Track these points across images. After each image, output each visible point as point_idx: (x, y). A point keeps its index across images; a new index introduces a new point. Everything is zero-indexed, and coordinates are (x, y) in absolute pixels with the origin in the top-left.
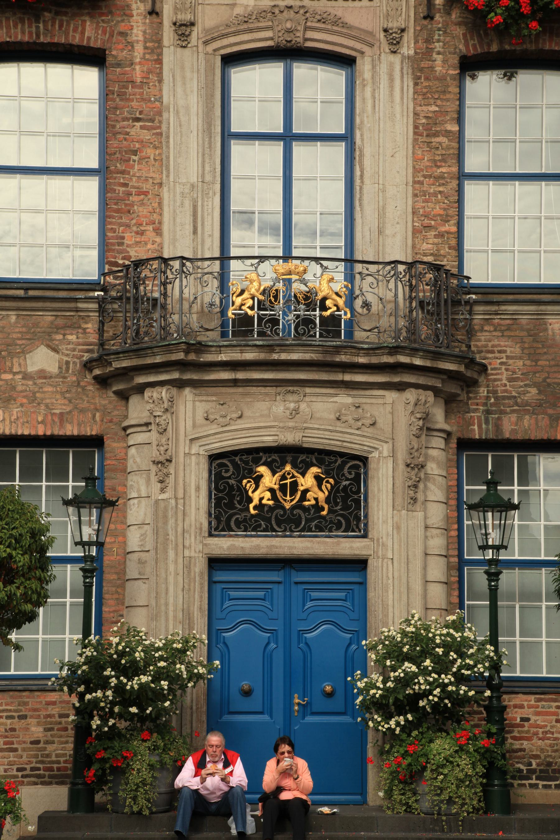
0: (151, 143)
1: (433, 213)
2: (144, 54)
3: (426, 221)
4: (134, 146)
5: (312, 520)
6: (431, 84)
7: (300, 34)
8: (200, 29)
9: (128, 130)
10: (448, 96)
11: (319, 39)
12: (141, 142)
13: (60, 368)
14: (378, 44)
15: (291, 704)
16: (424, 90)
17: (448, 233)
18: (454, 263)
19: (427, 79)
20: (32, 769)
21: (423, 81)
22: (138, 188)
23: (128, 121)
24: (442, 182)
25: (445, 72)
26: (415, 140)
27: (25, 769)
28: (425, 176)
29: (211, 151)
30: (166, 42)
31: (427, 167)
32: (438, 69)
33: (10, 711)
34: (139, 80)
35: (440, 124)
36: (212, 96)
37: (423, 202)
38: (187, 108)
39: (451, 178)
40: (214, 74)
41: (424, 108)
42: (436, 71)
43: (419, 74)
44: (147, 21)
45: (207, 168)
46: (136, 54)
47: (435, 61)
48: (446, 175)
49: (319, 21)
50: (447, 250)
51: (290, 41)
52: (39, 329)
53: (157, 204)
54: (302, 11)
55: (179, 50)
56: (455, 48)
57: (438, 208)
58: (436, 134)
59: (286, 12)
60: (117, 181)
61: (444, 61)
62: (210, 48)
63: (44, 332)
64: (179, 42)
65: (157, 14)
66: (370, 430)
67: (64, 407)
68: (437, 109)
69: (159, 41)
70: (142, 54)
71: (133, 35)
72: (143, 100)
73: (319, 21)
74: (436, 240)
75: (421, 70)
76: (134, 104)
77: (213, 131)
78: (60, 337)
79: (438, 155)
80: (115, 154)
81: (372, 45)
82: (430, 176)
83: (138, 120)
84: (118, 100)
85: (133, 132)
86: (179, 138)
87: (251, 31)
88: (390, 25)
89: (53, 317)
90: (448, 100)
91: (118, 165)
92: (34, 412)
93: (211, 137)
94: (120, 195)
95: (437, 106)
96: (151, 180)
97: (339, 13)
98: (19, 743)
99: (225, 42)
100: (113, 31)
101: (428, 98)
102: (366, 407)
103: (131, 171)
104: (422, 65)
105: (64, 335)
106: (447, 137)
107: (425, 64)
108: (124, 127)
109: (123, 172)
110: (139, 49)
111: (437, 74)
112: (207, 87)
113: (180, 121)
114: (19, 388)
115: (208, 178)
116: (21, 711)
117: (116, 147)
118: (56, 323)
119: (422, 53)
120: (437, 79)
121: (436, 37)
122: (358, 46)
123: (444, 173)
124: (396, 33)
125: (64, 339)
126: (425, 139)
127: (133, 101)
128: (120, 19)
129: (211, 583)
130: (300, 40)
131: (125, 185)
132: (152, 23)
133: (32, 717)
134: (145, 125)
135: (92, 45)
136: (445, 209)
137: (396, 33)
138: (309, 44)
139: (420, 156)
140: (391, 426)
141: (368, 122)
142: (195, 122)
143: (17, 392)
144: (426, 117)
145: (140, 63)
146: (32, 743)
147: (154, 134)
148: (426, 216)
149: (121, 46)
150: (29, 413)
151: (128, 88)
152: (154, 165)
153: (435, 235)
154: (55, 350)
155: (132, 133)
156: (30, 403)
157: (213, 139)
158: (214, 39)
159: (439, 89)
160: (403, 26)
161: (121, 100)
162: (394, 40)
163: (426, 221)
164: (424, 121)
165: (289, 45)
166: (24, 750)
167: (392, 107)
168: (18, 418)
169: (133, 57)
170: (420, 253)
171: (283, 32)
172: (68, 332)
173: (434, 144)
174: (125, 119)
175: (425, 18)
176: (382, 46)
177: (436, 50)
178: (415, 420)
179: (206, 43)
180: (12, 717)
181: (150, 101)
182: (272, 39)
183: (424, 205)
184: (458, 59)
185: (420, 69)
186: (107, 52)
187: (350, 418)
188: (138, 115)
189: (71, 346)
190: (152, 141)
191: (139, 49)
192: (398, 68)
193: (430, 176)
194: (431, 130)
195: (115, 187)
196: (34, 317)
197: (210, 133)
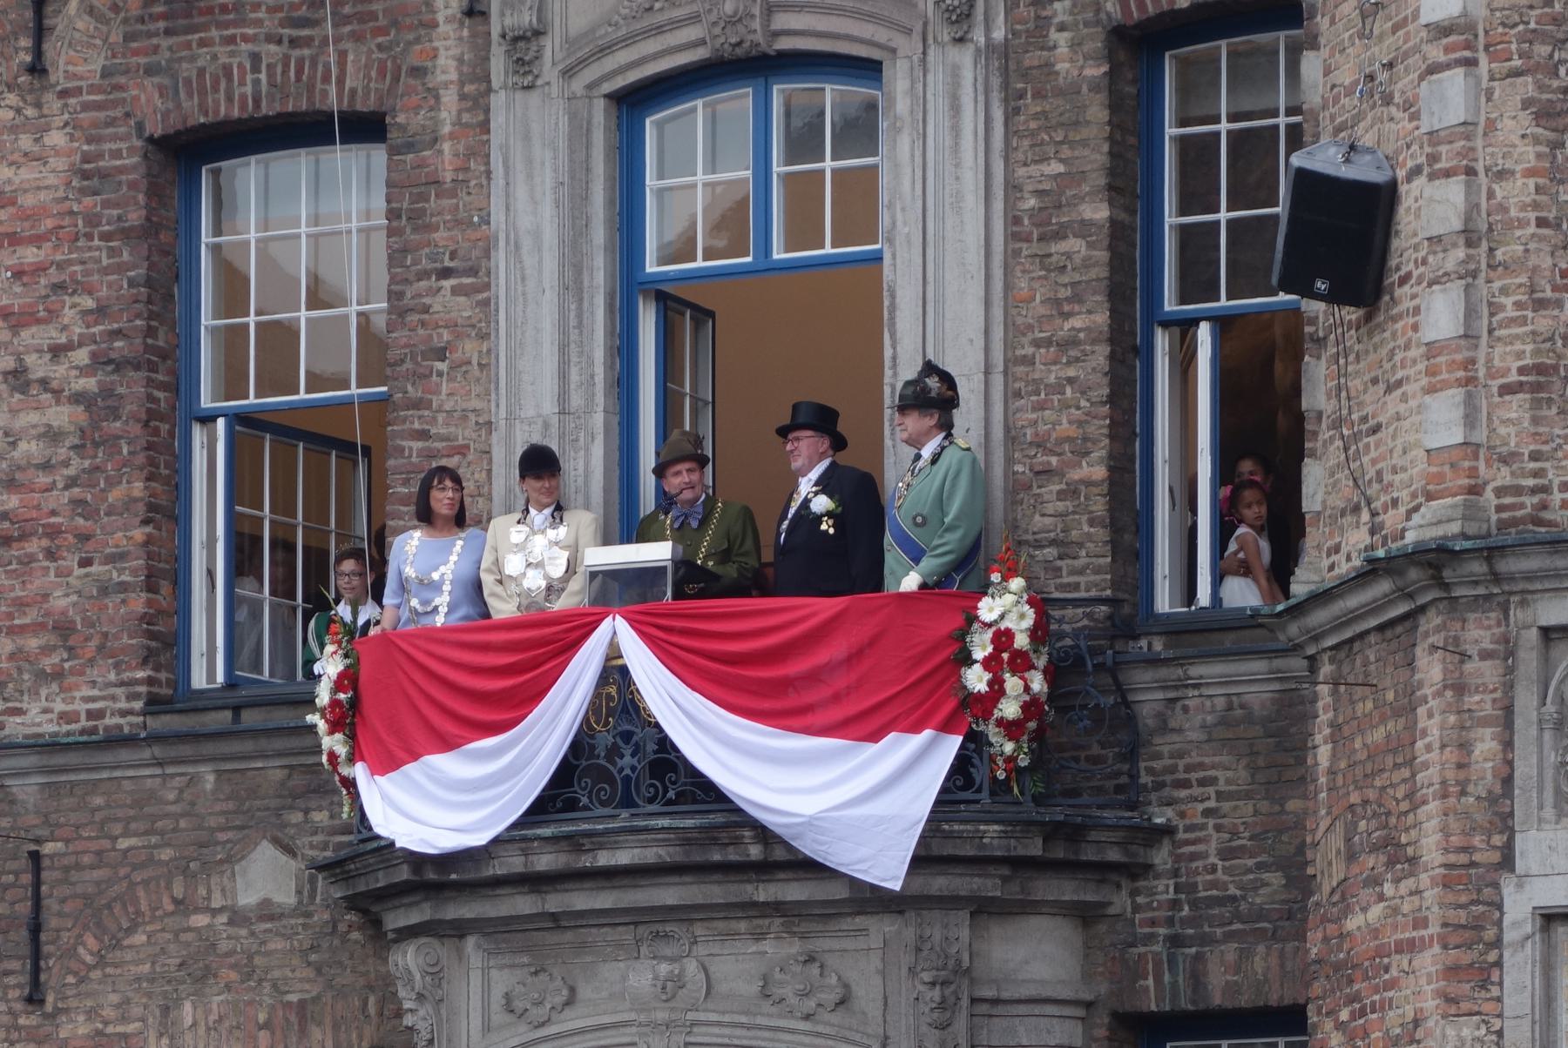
0: (473, 326)
1: (1054, 435)
2: (460, 112)
3: (1041, 458)
4: (440, 336)
6: (1048, 107)
7: (756, 24)
9: (427, 300)
10: (1085, 133)
12: (452, 325)
13: (299, 892)
14: (918, 27)
16: (1033, 125)
17: (1089, 483)
18: (1101, 561)
19: (1038, 95)
22: (448, 439)
23: (429, 278)
24: (1073, 353)
25: (1076, 73)
26: (1011, 256)
28: (1037, 344)
29: (581, 333)
30: (497, 79)
31: (1040, 319)
32: (1062, 67)
34: (448, 177)
35: (1069, 205)
36: (586, 198)
37: (1034, 409)
38: (537, 234)
39: (1094, 342)
40: (588, 146)
41: (1034, 170)
42: (1057, 73)
43: (1020, 86)
44: (465, 33)
45: (574, 376)
46: (444, 114)
47: (1055, 47)
48: (1082, 335)
50: (1086, 528)
51: (739, 44)
52: (258, 802)
53: (484, 474)
55: (519, 95)
56: (1098, 11)
57: (1064, 421)
58: (1059, 235)
60: (407, 426)
61: (1074, 45)
62: (578, 85)
63: (268, 809)
65: (483, 14)
66: (835, 1018)
67: (307, 987)
68: (1061, 168)
70: (454, 113)
71: (438, 72)
72: (458, 222)
74: (1061, 506)
76: (440, 236)
77: (586, 283)
78: (297, 817)
79: (1065, 285)
80: (403, 361)
81: (908, 32)
82: (1048, 342)
83: (446, 273)
84: (408, 230)
85: (437, 304)
86: (520, 308)
87: (659, 30)
89: (286, 771)
90: (1084, 143)
91: (410, 388)
92: (250, 1003)
93: (581, 300)
94: (414, 459)
95: (1061, 161)
100: (399, 68)
101: (1042, 143)
102: (831, 961)
103: (434, 398)
104: (1027, 63)
105: (306, 812)
106: (1084, 237)
107: (1033, 58)
108: (420, 296)
109: (417, 405)
110: (449, 98)
111: (1061, 80)
112: (572, 178)
113: (522, 269)
114: (224, 946)
115: (576, 400)
117: (406, 346)
118: (291, 783)
119: (1027, 31)
120: (1060, 92)
123: (1079, 330)
125: (306, 821)
126: (1036, 248)
127: (437, 229)
128: (411, 37)
130: (759, 37)
131: (423, 435)
132: (473, 35)
134: (460, 285)
135: (359, 107)
136: (1080, 423)
138: (785, 44)
139: (1025, 293)
140: (880, 1003)
141: (905, 224)
142: (546, 267)
143: (218, 956)
144: (1039, 193)
145: (452, 136)
147: (479, 303)
148: (1040, 444)
149: (415, 99)
150: (241, 1005)
151: (428, 201)
152: (478, 380)
153: (1059, 492)
154: (290, 851)
155: (436, 307)
156: (243, 982)
157: (586, 304)
158: (583, 63)
161: (415, 230)
163: (1041, 458)
164: (1032, 202)
165: (739, 52)
167: (957, 178)
168: (221, 1019)
169: (437, 123)
170: (1027, 542)
172: (313, 804)
173: (1054, 259)
174: (423, 275)
176: (930, 28)
178: (921, 988)
179: (568, 73)
181: (471, 222)
183: (1034, 416)
184: (1103, 37)
185: (1016, 76)
186: (388, 120)
187: (787, 992)
188: (448, 263)
189: (319, 838)
190: (474, 321)
191: (449, 98)
192: (968, 76)
193: (1048, 342)
194: (1050, 224)
195: (404, 443)
196: (250, 774)
197: (580, 290)
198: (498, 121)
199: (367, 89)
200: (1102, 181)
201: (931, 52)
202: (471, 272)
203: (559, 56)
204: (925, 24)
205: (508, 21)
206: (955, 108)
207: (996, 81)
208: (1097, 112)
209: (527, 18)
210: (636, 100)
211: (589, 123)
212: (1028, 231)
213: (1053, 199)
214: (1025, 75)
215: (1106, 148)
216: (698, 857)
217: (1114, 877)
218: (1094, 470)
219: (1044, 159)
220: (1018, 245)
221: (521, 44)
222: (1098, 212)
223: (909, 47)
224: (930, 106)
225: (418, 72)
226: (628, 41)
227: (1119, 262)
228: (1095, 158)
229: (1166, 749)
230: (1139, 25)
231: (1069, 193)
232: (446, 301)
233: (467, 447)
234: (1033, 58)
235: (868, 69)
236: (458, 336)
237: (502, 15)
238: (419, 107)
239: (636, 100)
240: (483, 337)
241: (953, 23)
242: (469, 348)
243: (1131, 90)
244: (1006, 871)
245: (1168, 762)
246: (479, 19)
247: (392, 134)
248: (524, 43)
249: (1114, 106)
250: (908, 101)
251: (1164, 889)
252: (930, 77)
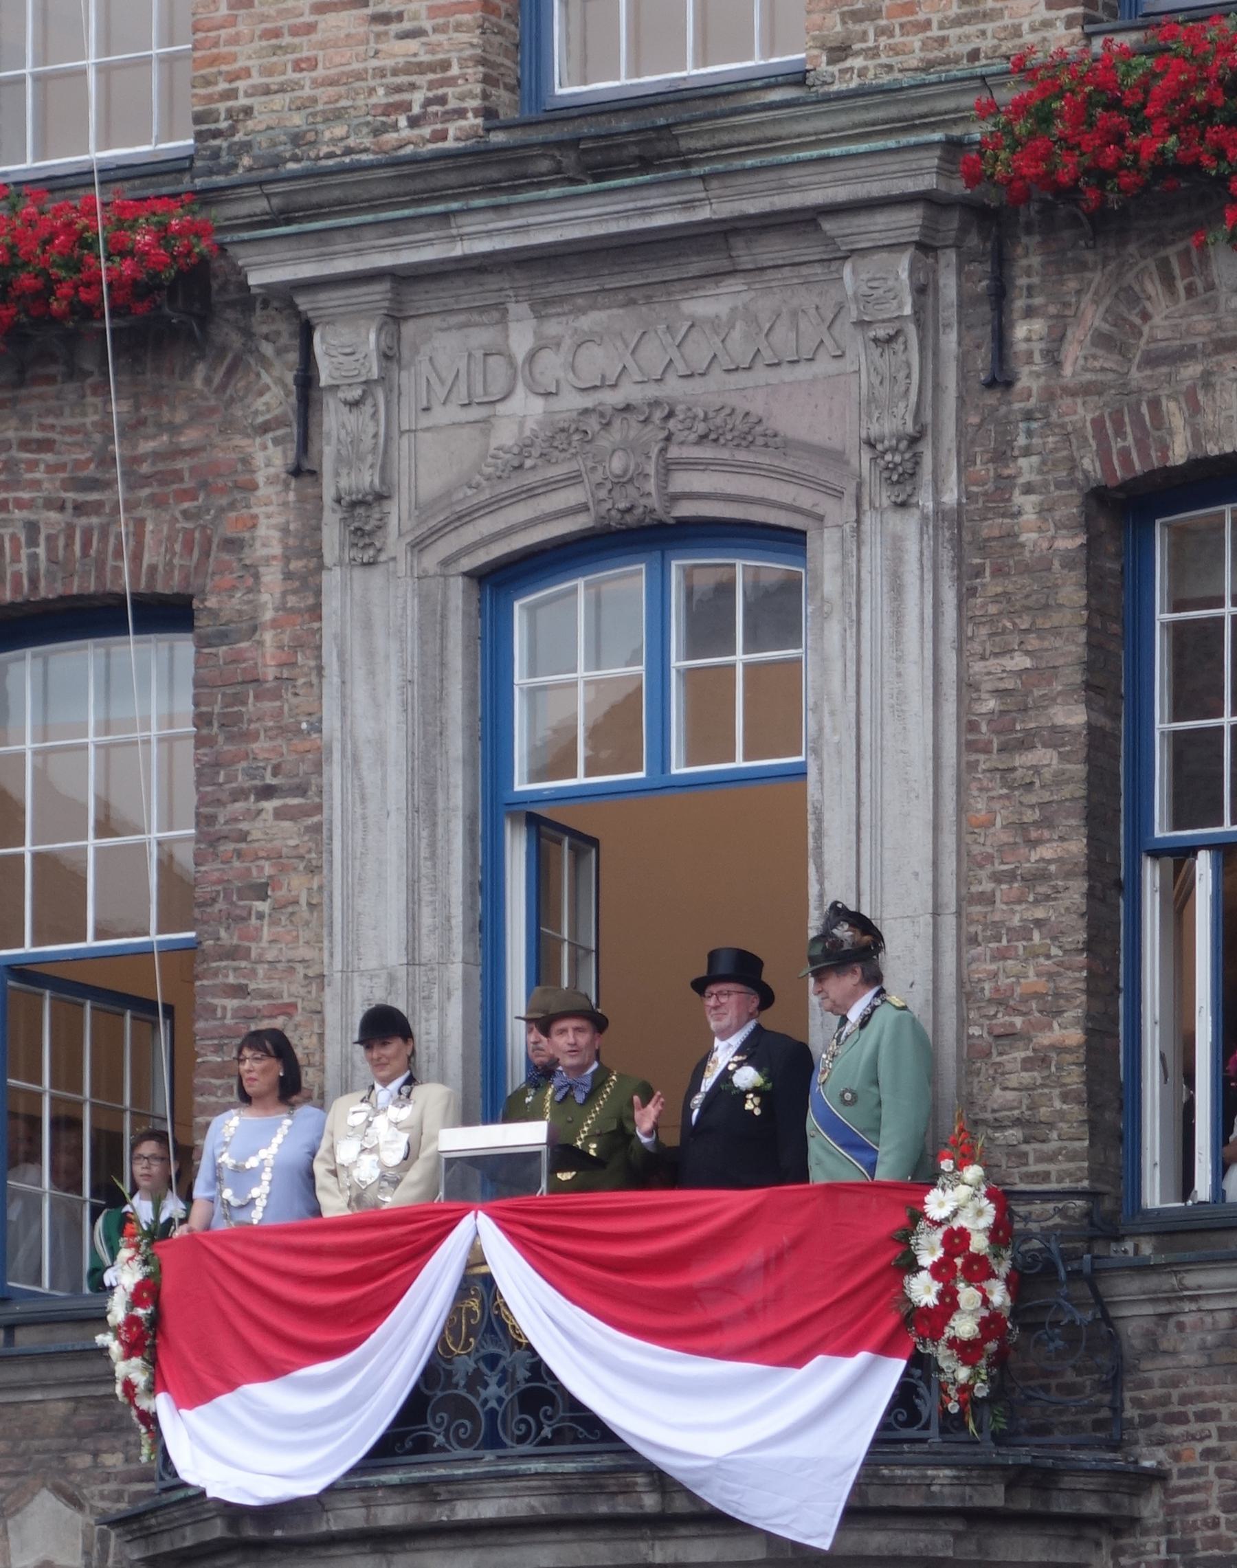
0: (302, 857)
1: (1018, 990)
2: (284, 594)
3: (1002, 1019)
4: (261, 869)
6: (1010, 588)
7: (651, 486)
8: (405, 506)
9: (244, 826)
10: (1056, 619)
11: (709, 487)
12: (276, 857)
13: (87, 1553)
14: (851, 489)
16: (993, 609)
17: (1061, 1049)
18: (1077, 1144)
19: (998, 572)
21: (987, 579)
23: (247, 799)
24: (1042, 889)
25: (1045, 545)
26: (966, 770)
28: (997, 878)
29: (434, 866)
30: (330, 553)
31: (1001, 848)
32: (1028, 537)
34: (271, 673)
35: (1037, 708)
36: (440, 699)
37: (994, 959)
38: (379, 744)
39: (1068, 875)
40: (443, 636)
41: (993, 664)
42: (1022, 546)
43: (978, 561)
44: (292, 496)
45: (426, 919)
46: (265, 597)
47: (1020, 513)
48: (1053, 868)
50: (1058, 1104)
51: (629, 510)
52: (37, 1443)
53: (315, 1039)
54: (658, 415)
55: (358, 573)
56: (1073, 469)
57: (1031, 973)
58: (1024, 744)
59: (617, 423)
60: (220, 980)
61: (1044, 511)
62: (430, 561)
65: (313, 473)
68: (1027, 663)
69: (317, 552)
70: (278, 595)
71: (258, 544)
72: (282, 730)
74: (1026, 1077)
75: (982, 547)
76: (260, 746)
77: (441, 805)
78: (84, 1461)
79: (1032, 807)
80: (214, 900)
81: (838, 494)
82: (1011, 876)
83: (267, 792)
84: (221, 739)
85: (256, 829)
86: (359, 835)
87: (530, 493)
88: (875, 430)
89: (71, 1405)
90: (1056, 631)
91: (223, 933)
93: (434, 824)
94: (229, 1021)
95: (1027, 653)
96: (300, 969)
97: (757, 407)
99: (470, 534)
100: (209, 541)
101: (1004, 630)
103: (253, 945)
104: (985, 533)
105: (96, 1454)
106: (1055, 747)
107: (992, 527)
108: (236, 820)
109: (233, 953)
110: (272, 577)
111: (1027, 554)
112: (423, 675)
113: (362, 787)
115: (429, 949)
117: (220, 882)
118: (76, 1419)
119: (985, 494)
120: (1026, 569)
121: (1022, 441)
123: (1049, 862)
124: (894, 450)
125: (96, 1465)
126: (996, 760)
127: (255, 737)
128: (224, 501)
130: (654, 502)
131: (239, 991)
132: (302, 499)
134: (285, 806)
135: (160, 588)
136: (1051, 976)
137: (894, 450)
138: (686, 510)
139: (982, 816)
141: (834, 730)
142: (391, 785)
144: (999, 693)
145: (275, 624)
147: (308, 829)
148: (1001, 1001)
149: (229, 578)
151: (244, 703)
152: (307, 923)
153: (1024, 1060)
154: (74, 1501)
155: (256, 835)
157: (440, 830)
158: (436, 533)
159: (1030, 602)
160: (910, 428)
161: (230, 738)
162: (901, 468)
163: (1002, 1019)
164: (991, 704)
165: (629, 519)
167: (899, 675)
169: (257, 607)
170: (984, 1122)
171: (609, 486)
172: (104, 1445)
174: (239, 795)
175: (991, 384)
176: (865, 490)
177: (1021, 480)
179: (419, 546)
181: (300, 731)
182: (584, 508)
183: (994, 967)
184: (1078, 501)
185: (972, 549)
186: (196, 603)
188: (270, 780)
189: (111, 1486)
190: (302, 851)
191: (272, 577)
192: (912, 548)
193: (1011, 876)
195: (216, 1001)
196: (25, 1408)
197: (433, 814)
198: (331, 604)
199: (170, 564)
200: (1079, 678)
201: (867, 520)
202: (299, 791)
203: (407, 525)
204: (860, 486)
205: (344, 483)
206: (897, 589)
207: (947, 556)
208: (1072, 593)
209: (366, 479)
210: (502, 579)
211: (444, 607)
212: (987, 738)
213: (1017, 700)
214: (982, 547)
215: (1082, 637)
216: (579, 1509)
217: (1092, 1533)
218: (1068, 1032)
219: (1007, 652)
220: (973, 757)
221: (360, 511)
222: (1073, 716)
223: (838, 512)
224: (866, 585)
225: (233, 545)
227: (1099, 779)
228: (1070, 649)
229: (1156, 1376)
230: (1123, 486)
231: (1037, 693)
232: (268, 827)
233: (294, 1005)
234: (992, 527)
235: (790, 540)
236: (283, 869)
237: (337, 474)
238: (234, 588)
239: (502, 579)
240: (314, 870)
241: (893, 484)
242: (297, 885)
243: (1112, 566)
244: (958, 1525)
245: (1159, 1391)
246: (308, 480)
247: (201, 622)
248: (364, 508)
249: (1094, 586)
250: (838, 580)
251: (1155, 1547)
252: (866, 551)
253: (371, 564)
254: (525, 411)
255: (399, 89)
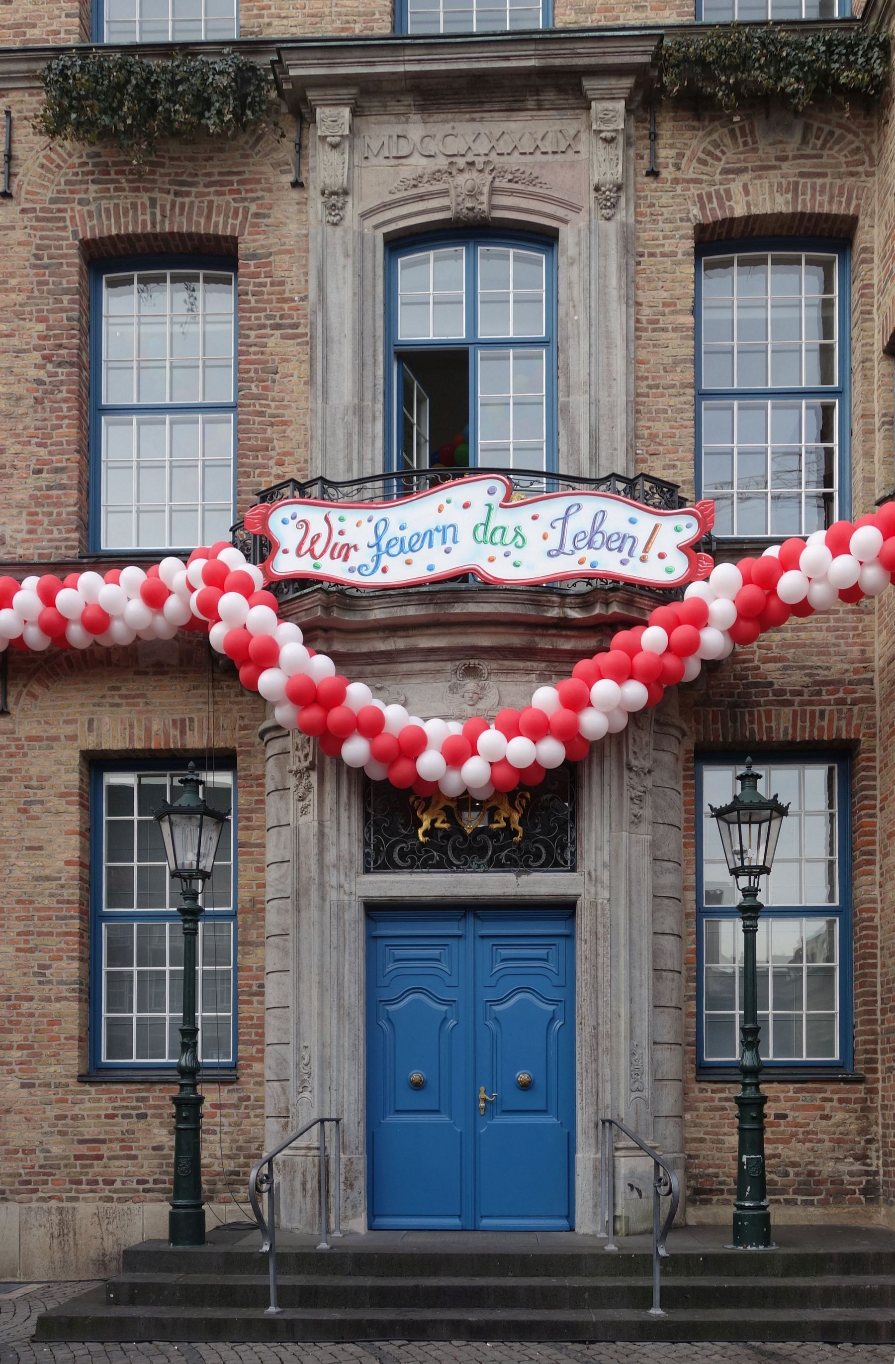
5: (502, 849)
7: (484, 198)
15: (476, 1100)
20: (156, 1182)
27: (146, 1182)
33: (127, 1107)
49: (510, 181)
64: (331, 219)
73: (510, 181)
87: (421, 198)
98: (138, 1148)
116: (140, 1108)
122: (561, 212)
129: (371, 938)
130: (485, 207)
133: (154, 1116)
146: (155, 1148)
165: (471, 214)
166: (146, 1157)
171: (463, 196)
179: (364, 216)
180: (129, 1116)
182: (448, 208)
226: (405, 201)
253: (335, 224)
254: (418, 163)
255: (348, 22)
